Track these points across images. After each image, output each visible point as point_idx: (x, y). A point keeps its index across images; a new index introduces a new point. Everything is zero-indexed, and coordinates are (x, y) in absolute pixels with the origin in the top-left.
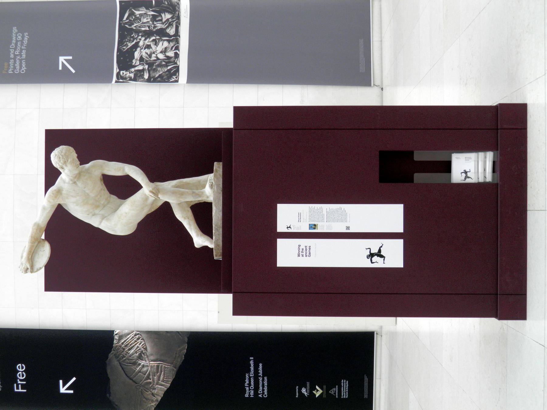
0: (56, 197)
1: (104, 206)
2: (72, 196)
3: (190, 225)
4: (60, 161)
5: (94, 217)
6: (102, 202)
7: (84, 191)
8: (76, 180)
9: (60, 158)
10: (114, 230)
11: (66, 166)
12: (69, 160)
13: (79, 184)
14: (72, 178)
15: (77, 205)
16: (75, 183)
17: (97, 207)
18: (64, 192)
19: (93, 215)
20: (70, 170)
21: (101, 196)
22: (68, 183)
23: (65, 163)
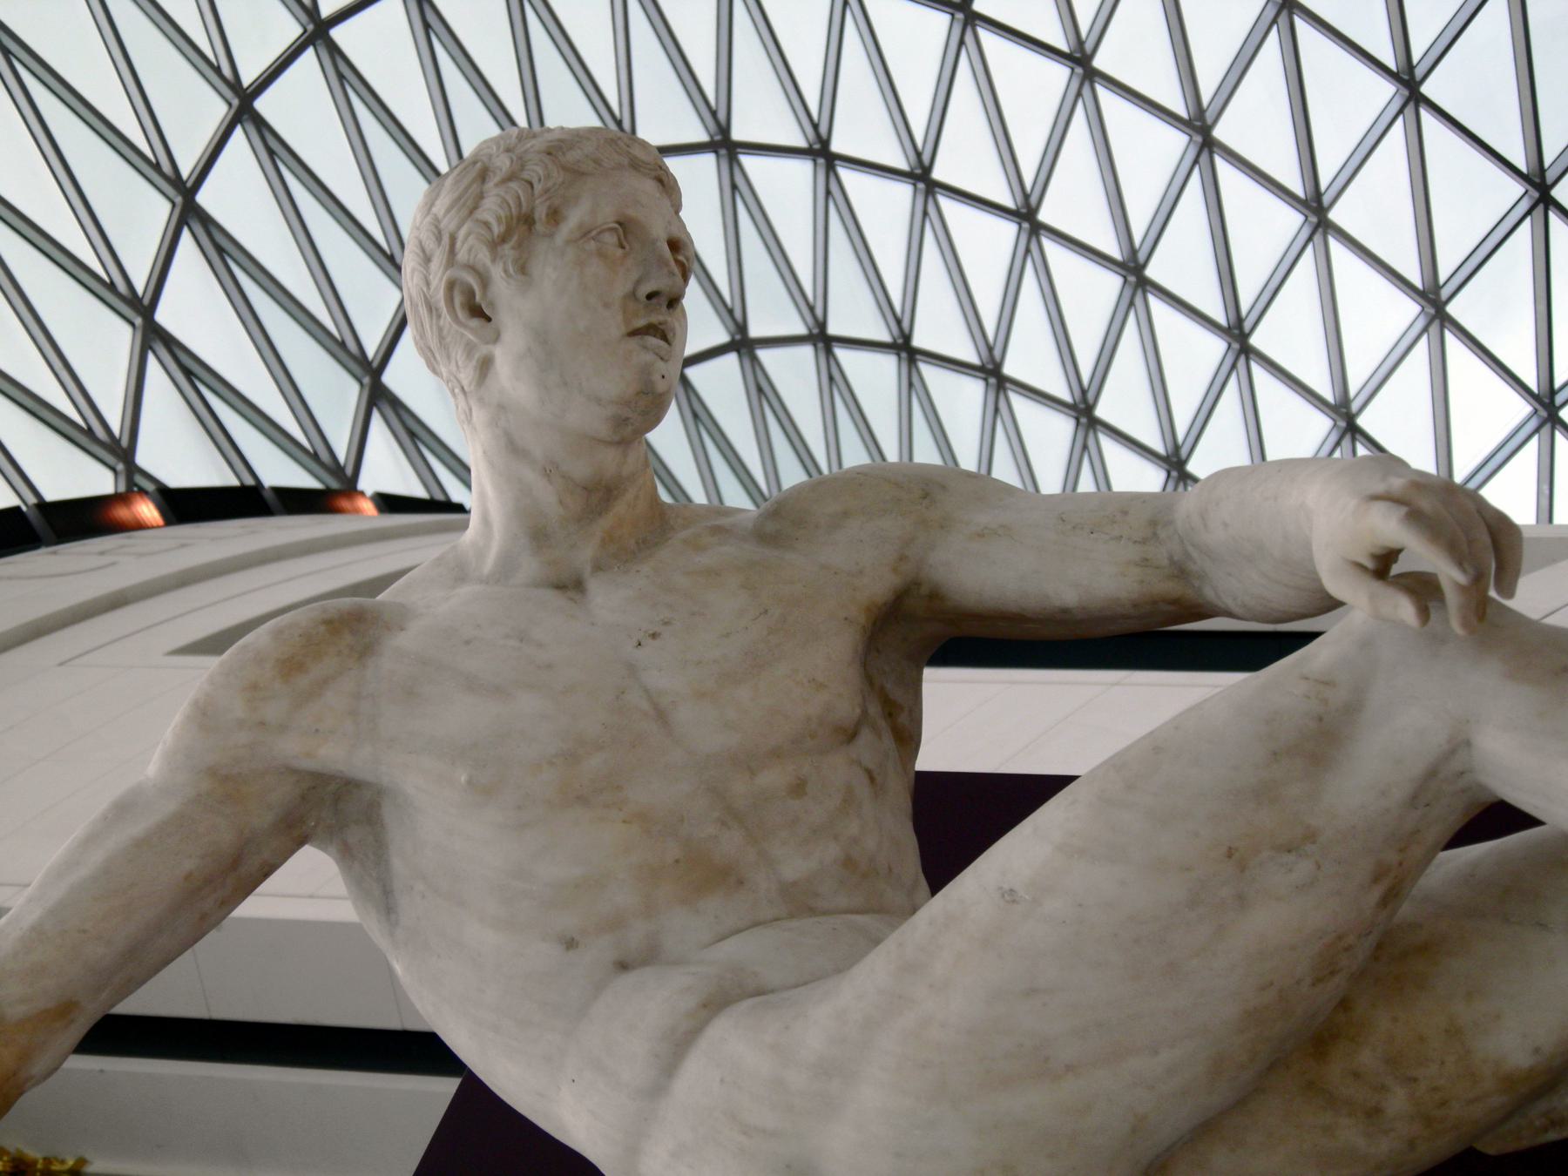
0: (291, 666)
1: (799, 902)
4: (471, 213)
5: (630, 978)
6: (794, 865)
7: (632, 669)
8: (585, 554)
9: (483, 176)
11: (523, 269)
12: (575, 217)
13: (609, 599)
14: (547, 495)
16: (571, 586)
17: (707, 876)
18: (405, 640)
19: (623, 966)
20: (546, 354)
21: (798, 788)
23: (522, 230)
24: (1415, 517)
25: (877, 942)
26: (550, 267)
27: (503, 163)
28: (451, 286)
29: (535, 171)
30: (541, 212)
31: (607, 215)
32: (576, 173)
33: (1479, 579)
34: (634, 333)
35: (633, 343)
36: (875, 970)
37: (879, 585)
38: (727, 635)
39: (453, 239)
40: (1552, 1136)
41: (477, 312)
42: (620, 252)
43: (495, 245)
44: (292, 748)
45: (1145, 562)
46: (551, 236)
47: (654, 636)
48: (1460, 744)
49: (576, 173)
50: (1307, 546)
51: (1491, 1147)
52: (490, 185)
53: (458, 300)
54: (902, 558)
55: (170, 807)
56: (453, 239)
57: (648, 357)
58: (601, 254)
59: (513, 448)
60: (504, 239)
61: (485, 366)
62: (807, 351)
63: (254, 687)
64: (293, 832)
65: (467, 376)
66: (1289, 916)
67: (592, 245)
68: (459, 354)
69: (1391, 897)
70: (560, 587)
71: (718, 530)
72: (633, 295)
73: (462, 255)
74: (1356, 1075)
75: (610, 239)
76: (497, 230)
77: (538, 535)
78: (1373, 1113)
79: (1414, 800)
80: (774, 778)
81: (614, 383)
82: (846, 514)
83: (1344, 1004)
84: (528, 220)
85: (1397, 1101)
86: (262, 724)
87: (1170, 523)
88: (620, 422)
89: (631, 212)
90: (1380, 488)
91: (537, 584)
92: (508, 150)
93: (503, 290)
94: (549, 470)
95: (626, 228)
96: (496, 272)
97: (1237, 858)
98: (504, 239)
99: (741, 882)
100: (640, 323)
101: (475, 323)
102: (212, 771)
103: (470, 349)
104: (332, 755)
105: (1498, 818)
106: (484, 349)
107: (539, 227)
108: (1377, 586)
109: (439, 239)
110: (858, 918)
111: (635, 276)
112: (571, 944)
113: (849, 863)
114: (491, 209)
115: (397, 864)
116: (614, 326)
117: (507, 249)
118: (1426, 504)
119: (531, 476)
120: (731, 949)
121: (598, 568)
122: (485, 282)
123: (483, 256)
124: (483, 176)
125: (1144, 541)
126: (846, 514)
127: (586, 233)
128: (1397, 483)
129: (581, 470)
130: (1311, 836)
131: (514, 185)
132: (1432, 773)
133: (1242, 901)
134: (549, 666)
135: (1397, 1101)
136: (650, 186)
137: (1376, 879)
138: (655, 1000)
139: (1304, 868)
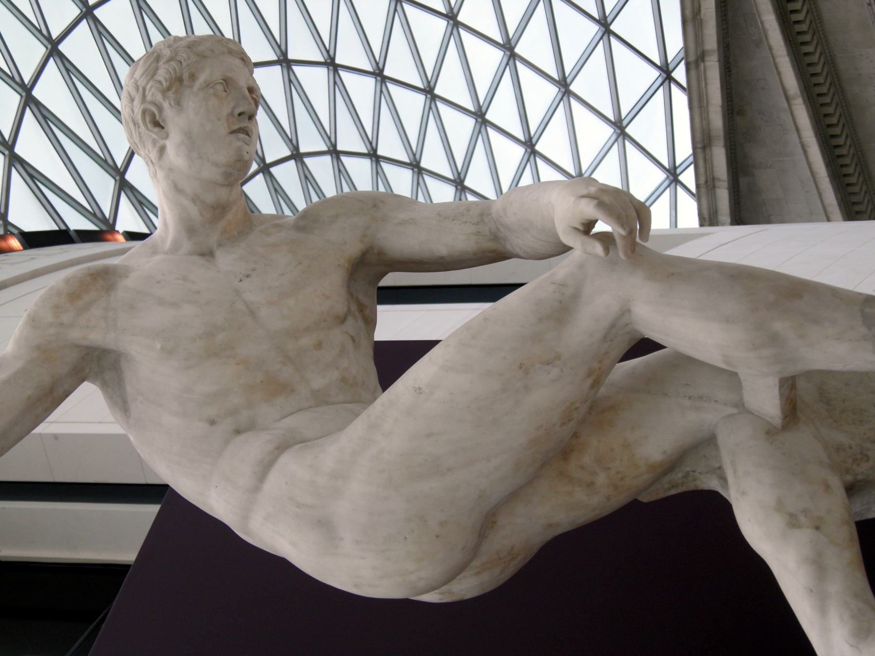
1: (321, 399)
2: (161, 302)
3: (818, 566)
6: (318, 383)
7: (238, 292)
8: (214, 238)
9: (158, 59)
10: (325, 526)
11: (178, 103)
12: (203, 77)
14: (194, 211)
15: (169, 352)
16: (208, 254)
17: (276, 388)
18: (129, 282)
19: (238, 432)
20: (191, 143)
21: (319, 345)
22: (176, 247)
23: (177, 84)
24: (601, 205)
25: (357, 415)
26: (191, 103)
27: (167, 53)
28: (144, 112)
29: (182, 56)
30: (186, 76)
31: (218, 75)
32: (202, 56)
33: (631, 232)
34: (233, 132)
35: (233, 137)
36: (357, 428)
37: (354, 249)
38: (283, 275)
39: (144, 89)
40: (673, 492)
41: (157, 124)
42: (224, 94)
43: (164, 92)
44: (75, 335)
45: (478, 234)
46: (191, 87)
47: (248, 276)
48: (625, 311)
49: (202, 56)
50: (552, 222)
51: (645, 498)
52: (161, 63)
53: (148, 119)
54: (365, 236)
55: (19, 365)
56: (144, 89)
57: (240, 144)
58: (215, 95)
59: (177, 189)
60: (169, 89)
61: (162, 150)
62: (277, 69)
63: (57, 307)
64: (78, 376)
65: (154, 155)
66: (549, 395)
67: (211, 91)
68: (149, 145)
69: (597, 383)
70: (202, 255)
71: (277, 226)
72: (231, 114)
73: (149, 97)
74: (582, 468)
75: (220, 88)
76: (165, 84)
77: (189, 229)
78: (590, 485)
79: (605, 338)
80: (306, 341)
81: (224, 156)
82: (337, 216)
83: (576, 435)
84: (180, 80)
85: (601, 479)
86: (62, 324)
87: (490, 214)
88: (227, 175)
89: (229, 75)
90: (585, 192)
91: (191, 254)
92: (169, 46)
93: (169, 113)
94: (195, 199)
95: (227, 82)
96: (166, 105)
97: (524, 368)
98: (169, 89)
99: (293, 391)
100: (236, 127)
101: (156, 130)
102: (38, 348)
103: (154, 142)
104: (95, 338)
105: (644, 346)
106: (161, 142)
107: (186, 83)
108: (584, 238)
109: (137, 89)
110: (349, 406)
111: (232, 104)
112: (212, 422)
113: (343, 380)
114: (162, 74)
115: (129, 389)
116: (223, 130)
117: (170, 94)
118: (606, 199)
119: (186, 202)
120: (289, 422)
121: (220, 245)
122: (160, 109)
123: (159, 97)
124: (158, 59)
125: (478, 224)
126: (337, 216)
127: (208, 85)
128: (593, 190)
129: (210, 198)
130: (558, 357)
131: (172, 63)
132: (613, 326)
133: (527, 388)
134: (198, 292)
135: (601, 479)
136: (238, 62)
137: (589, 376)
138: (253, 447)
139: (555, 372)
